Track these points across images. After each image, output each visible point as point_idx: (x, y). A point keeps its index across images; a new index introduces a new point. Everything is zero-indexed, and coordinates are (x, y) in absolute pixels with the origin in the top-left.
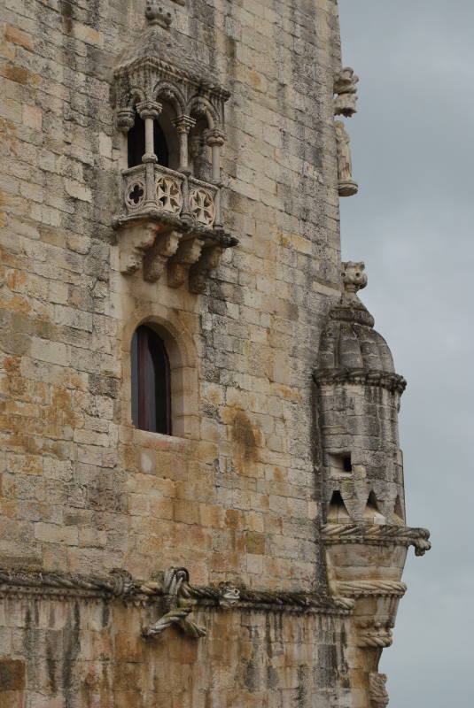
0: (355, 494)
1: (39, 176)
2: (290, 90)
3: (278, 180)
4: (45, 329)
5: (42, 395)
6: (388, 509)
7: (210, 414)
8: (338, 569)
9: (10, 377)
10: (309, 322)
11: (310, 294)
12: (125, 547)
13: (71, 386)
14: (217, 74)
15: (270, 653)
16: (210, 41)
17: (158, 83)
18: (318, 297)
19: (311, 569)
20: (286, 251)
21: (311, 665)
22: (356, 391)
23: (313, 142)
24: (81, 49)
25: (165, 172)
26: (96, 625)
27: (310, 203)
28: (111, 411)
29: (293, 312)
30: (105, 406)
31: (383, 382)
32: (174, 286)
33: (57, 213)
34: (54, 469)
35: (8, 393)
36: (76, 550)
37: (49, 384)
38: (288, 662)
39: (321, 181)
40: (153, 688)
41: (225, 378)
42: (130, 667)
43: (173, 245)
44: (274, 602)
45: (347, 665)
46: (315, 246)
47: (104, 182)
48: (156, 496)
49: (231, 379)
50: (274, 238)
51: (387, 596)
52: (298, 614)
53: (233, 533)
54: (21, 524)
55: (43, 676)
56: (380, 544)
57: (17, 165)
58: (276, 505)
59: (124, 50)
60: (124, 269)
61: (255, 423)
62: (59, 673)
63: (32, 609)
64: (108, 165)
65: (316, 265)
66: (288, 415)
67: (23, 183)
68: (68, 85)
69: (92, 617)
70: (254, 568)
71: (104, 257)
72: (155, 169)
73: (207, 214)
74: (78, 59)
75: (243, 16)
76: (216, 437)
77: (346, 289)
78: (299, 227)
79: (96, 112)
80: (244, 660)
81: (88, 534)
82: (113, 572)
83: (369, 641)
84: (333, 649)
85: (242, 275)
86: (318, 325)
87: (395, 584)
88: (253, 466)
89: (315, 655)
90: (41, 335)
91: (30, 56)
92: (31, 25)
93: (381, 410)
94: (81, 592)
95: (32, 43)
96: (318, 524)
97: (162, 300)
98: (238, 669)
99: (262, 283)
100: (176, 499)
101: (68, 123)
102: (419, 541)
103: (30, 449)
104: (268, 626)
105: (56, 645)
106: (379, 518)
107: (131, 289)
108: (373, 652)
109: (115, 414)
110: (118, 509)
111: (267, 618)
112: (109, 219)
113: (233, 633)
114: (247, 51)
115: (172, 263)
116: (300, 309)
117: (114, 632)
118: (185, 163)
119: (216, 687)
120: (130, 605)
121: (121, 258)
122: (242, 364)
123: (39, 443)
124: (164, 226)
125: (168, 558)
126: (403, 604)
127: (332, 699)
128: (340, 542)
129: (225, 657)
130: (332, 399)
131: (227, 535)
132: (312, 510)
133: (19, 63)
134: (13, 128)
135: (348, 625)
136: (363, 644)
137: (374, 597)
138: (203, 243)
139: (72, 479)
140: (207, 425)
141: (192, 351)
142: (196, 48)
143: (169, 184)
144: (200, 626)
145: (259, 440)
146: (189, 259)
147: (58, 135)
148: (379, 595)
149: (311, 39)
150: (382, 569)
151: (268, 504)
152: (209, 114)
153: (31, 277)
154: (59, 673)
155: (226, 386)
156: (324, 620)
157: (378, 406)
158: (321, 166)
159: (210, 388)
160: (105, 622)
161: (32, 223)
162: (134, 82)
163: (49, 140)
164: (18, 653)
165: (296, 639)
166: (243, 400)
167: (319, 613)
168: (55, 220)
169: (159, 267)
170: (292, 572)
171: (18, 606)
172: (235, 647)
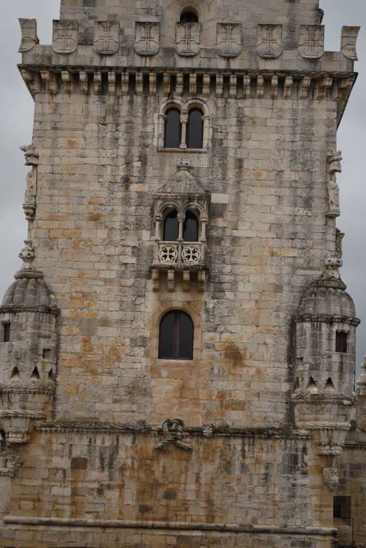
1: (106, 259)
3: (272, 222)
4: (105, 323)
5: (103, 351)
6: (321, 385)
7: (209, 348)
9: (85, 346)
10: (292, 292)
13: (119, 344)
14: (227, 180)
15: (244, 457)
16: (224, 167)
17: (162, 204)
18: (302, 278)
20: (275, 258)
21: (276, 464)
22: (307, 325)
24: (134, 195)
25: (165, 244)
27: (299, 228)
30: (140, 351)
31: (320, 320)
34: (106, 380)
35: (83, 352)
36: (123, 414)
37: (107, 346)
39: (310, 214)
40: (161, 470)
41: (221, 328)
42: (149, 462)
43: (171, 275)
45: (306, 465)
47: (145, 252)
48: (169, 388)
50: (266, 253)
52: (265, 439)
53: (222, 402)
54: (88, 404)
55: (97, 463)
57: (93, 256)
58: (255, 386)
61: (242, 348)
64: (147, 244)
65: (300, 261)
66: (270, 341)
68: (125, 214)
69: (126, 441)
71: (143, 285)
72: (159, 244)
74: (131, 201)
76: (213, 358)
77: (327, 268)
79: (141, 221)
81: (126, 406)
86: (300, 292)
88: (239, 369)
89: (280, 459)
90: (102, 325)
91: (103, 208)
92: (104, 193)
93: (320, 334)
94: (117, 430)
95: (104, 202)
96: (288, 393)
97: (178, 299)
98: (220, 463)
99: (252, 279)
100: (182, 388)
103: (94, 373)
104: (243, 444)
105: (105, 452)
107: (159, 297)
109: (145, 354)
110: (145, 395)
111: (243, 441)
113: (217, 448)
114: (254, 162)
117: (139, 447)
118: (180, 236)
119: (204, 471)
121: (151, 285)
123: (100, 370)
125: (175, 414)
129: (211, 459)
131: (217, 403)
132: (285, 387)
133: (96, 213)
135: (308, 444)
138: (188, 271)
140: (205, 352)
141: (200, 319)
142: (213, 171)
143: (168, 249)
145: (245, 356)
147: (117, 237)
149: (308, 137)
150: (319, 416)
151: (250, 386)
154: (106, 462)
157: (318, 332)
158: (311, 206)
159: (208, 336)
160: (134, 442)
161: (100, 279)
164: (85, 455)
165: (265, 450)
166: (232, 338)
167: (283, 438)
168: (113, 275)
171: (85, 437)
172: (219, 454)
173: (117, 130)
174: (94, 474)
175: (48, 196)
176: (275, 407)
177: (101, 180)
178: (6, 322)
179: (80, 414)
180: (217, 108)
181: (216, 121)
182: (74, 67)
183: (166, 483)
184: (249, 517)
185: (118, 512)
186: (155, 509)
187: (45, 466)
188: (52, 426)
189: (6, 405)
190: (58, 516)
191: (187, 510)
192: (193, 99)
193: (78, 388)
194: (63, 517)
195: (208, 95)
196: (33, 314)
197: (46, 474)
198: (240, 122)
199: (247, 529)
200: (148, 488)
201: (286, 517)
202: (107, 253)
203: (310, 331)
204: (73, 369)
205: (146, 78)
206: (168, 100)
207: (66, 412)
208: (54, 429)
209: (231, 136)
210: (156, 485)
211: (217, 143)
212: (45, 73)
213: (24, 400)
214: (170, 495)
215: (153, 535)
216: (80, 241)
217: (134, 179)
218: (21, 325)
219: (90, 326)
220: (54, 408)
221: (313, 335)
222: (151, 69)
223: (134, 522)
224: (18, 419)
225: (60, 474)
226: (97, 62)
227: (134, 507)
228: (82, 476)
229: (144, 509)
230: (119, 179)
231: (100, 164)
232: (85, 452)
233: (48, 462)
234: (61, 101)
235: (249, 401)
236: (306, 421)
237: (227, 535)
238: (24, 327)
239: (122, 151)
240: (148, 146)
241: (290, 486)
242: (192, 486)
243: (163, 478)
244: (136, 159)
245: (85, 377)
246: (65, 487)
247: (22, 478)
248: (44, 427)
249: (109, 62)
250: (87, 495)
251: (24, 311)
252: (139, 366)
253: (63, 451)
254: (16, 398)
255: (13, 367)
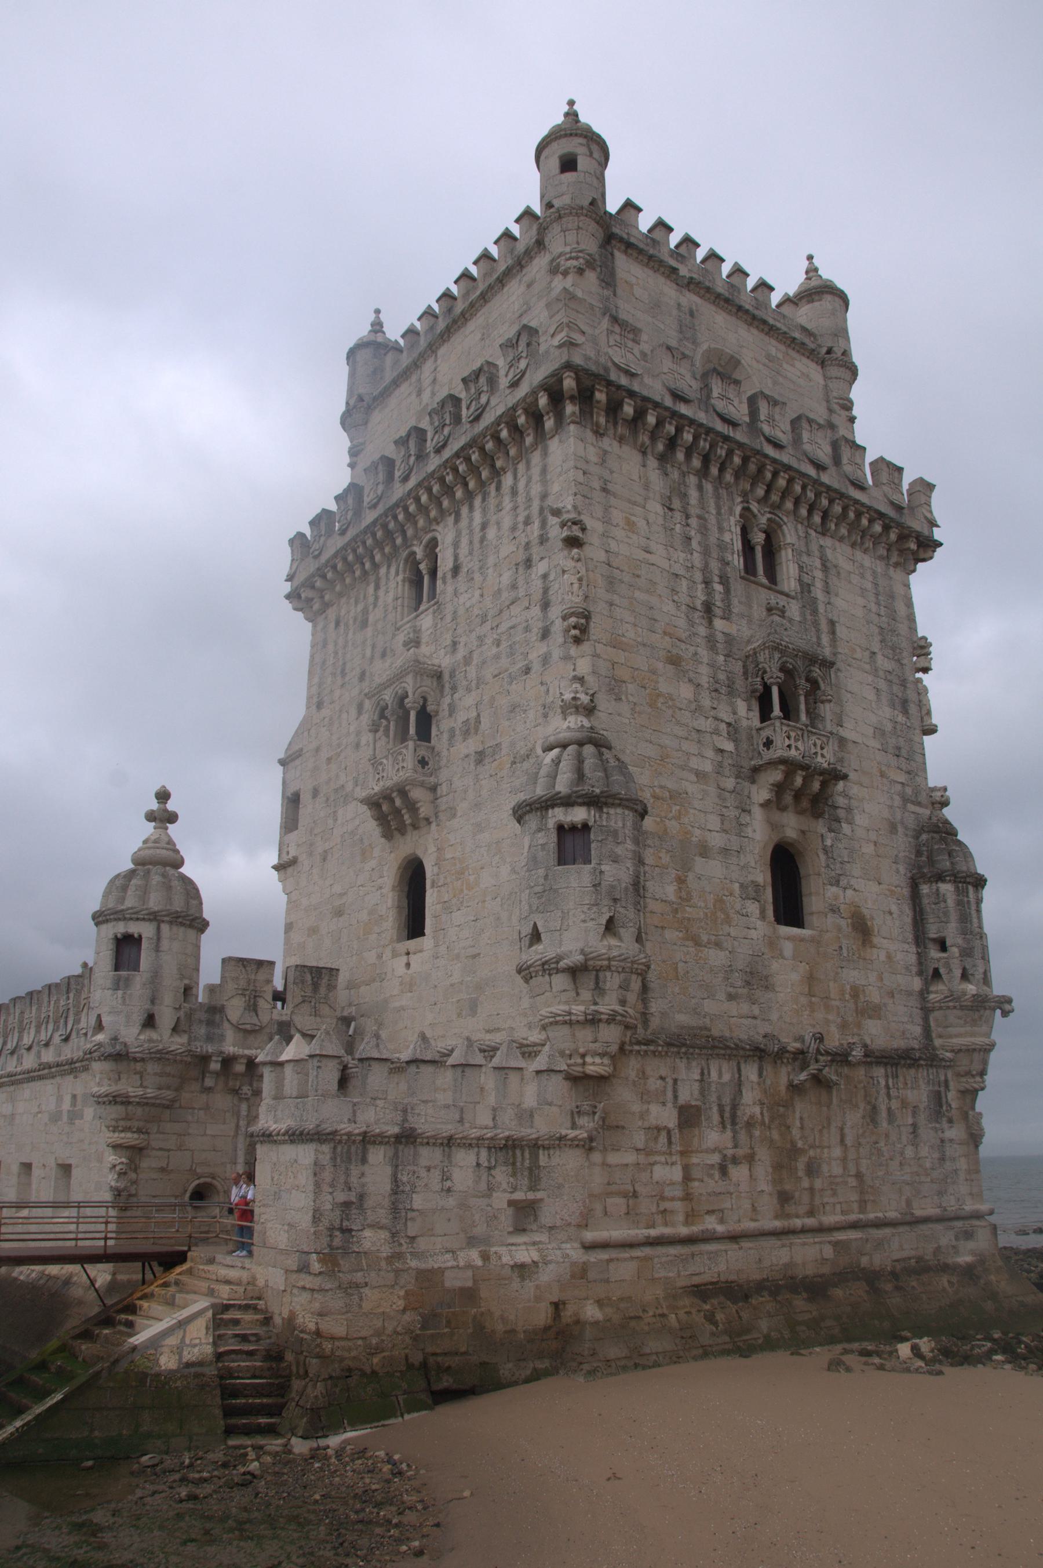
0: (951, 970)
1: (694, 735)
2: (879, 657)
4: (704, 851)
7: (833, 911)
8: (940, 1029)
9: (680, 888)
10: (907, 835)
11: (907, 814)
12: (774, 1016)
16: (816, 624)
19: (918, 1030)
21: (922, 1106)
22: (946, 888)
23: (900, 695)
26: (754, 1077)
27: (902, 742)
28: (758, 912)
29: (893, 828)
30: (753, 908)
31: (968, 880)
32: (801, 812)
33: (709, 762)
34: (717, 958)
36: (737, 1021)
38: (904, 1104)
41: (843, 882)
42: (782, 1109)
43: (799, 781)
44: (891, 1057)
45: (950, 1105)
46: (907, 776)
48: (795, 977)
49: (848, 883)
51: (980, 1050)
52: (910, 1066)
53: (856, 1003)
54: (693, 1001)
55: (716, 1118)
56: (971, 1009)
59: (752, 636)
60: (761, 801)
62: (727, 1115)
63: (706, 1067)
64: (745, 723)
65: (909, 791)
66: (894, 908)
67: (683, 741)
68: (712, 665)
69: (751, 1072)
70: (874, 1031)
71: (746, 793)
73: (823, 756)
75: (838, 602)
76: (839, 929)
78: (893, 761)
79: (733, 683)
80: (869, 1103)
81: (745, 1008)
82: (765, 1036)
83: (968, 1086)
84: (939, 1092)
85: (852, 801)
86: (913, 837)
87: (987, 1041)
88: (869, 950)
89: (924, 1098)
90: (702, 855)
91: (683, 646)
92: (682, 622)
93: (968, 902)
94: (742, 1052)
95: (683, 636)
96: (923, 994)
97: (791, 825)
100: (811, 979)
101: (713, 694)
102: (1004, 1005)
103: (697, 943)
104: (887, 1076)
106: (971, 988)
108: (971, 1094)
110: (767, 987)
112: (747, 764)
113: (860, 1082)
115: (798, 796)
116: (899, 825)
117: (768, 1082)
118: (803, 717)
119: (849, 1124)
120: (779, 1062)
121: (761, 793)
122: (856, 870)
123: (705, 938)
124: (790, 766)
126: (993, 1056)
127: (940, 1132)
128: (941, 1008)
130: (928, 895)
131: (851, 1005)
132: (917, 984)
133: (674, 651)
134: (673, 700)
136: (962, 1089)
137: (970, 1051)
139: (730, 966)
140: (831, 919)
143: (793, 734)
144: (834, 1078)
145: (873, 931)
146: (812, 791)
147: (707, 703)
148: (974, 1050)
149: (893, 616)
151: (882, 980)
152: (820, 679)
153: (692, 811)
154: (727, 1115)
155: (845, 888)
156: (931, 1071)
160: (760, 1075)
161: (691, 770)
162: (761, 659)
163: (700, 707)
164: (696, 1100)
168: (708, 767)
169: (788, 798)
170: (903, 1033)
171: (694, 1064)
173: (688, 525)
174: (713, 1137)
175: (607, 602)
176: (911, 1016)
177: (676, 598)
178: (573, 828)
179: (682, 1019)
180: (799, 537)
181: (800, 555)
182: (646, 399)
183: (806, 1147)
184: (904, 1198)
185: (750, 1206)
186: (797, 1194)
187: (640, 1123)
188: (648, 1043)
189: (586, 995)
190: (666, 1224)
191: (835, 1194)
192: (770, 513)
193: (676, 968)
194: (673, 1225)
195: (788, 513)
196: (631, 814)
197: (639, 1139)
198: (825, 568)
199: (908, 1218)
200: (786, 1158)
201: (940, 1193)
202: (696, 724)
203: (954, 897)
204: (666, 931)
205: (730, 453)
206: (742, 502)
207: (663, 1014)
208: (652, 1048)
209: (819, 584)
210: (794, 1152)
211: (806, 588)
212: (601, 391)
213: (624, 987)
214: (812, 1170)
215: (804, 1244)
216: (658, 695)
217: (718, 612)
218: (615, 833)
219: (689, 852)
220: (646, 1007)
221: (959, 903)
222: (741, 445)
223: (777, 1224)
224: (612, 1026)
225: (663, 1139)
226: (668, 402)
227: (770, 1194)
228: (696, 1141)
229: (784, 1198)
230: (698, 604)
231: (672, 571)
232: (696, 1093)
233: (643, 1115)
234: (609, 449)
235: (885, 1004)
236: (950, 1037)
237: (888, 1231)
238: (620, 834)
239: (697, 559)
240: (728, 564)
241: (938, 1142)
242: (837, 1152)
243: (800, 1138)
244: (716, 579)
245: (685, 949)
246: (673, 1164)
247: (605, 1149)
248: (639, 1043)
249: (683, 409)
250: (706, 1179)
251: (620, 805)
252: (753, 934)
253: (664, 1092)
254: (612, 981)
255: (606, 916)
